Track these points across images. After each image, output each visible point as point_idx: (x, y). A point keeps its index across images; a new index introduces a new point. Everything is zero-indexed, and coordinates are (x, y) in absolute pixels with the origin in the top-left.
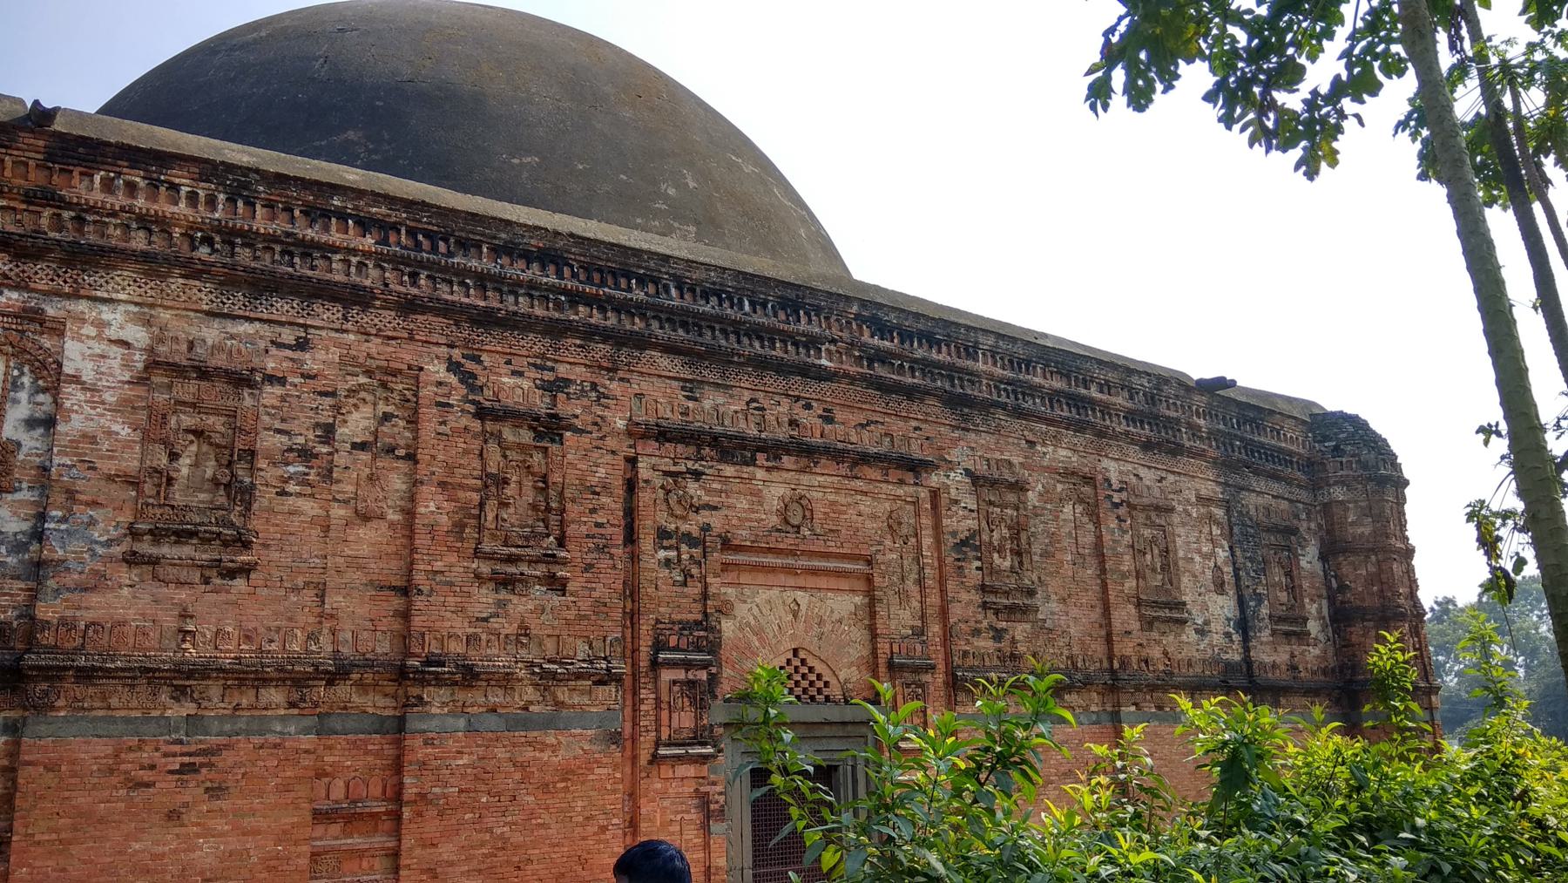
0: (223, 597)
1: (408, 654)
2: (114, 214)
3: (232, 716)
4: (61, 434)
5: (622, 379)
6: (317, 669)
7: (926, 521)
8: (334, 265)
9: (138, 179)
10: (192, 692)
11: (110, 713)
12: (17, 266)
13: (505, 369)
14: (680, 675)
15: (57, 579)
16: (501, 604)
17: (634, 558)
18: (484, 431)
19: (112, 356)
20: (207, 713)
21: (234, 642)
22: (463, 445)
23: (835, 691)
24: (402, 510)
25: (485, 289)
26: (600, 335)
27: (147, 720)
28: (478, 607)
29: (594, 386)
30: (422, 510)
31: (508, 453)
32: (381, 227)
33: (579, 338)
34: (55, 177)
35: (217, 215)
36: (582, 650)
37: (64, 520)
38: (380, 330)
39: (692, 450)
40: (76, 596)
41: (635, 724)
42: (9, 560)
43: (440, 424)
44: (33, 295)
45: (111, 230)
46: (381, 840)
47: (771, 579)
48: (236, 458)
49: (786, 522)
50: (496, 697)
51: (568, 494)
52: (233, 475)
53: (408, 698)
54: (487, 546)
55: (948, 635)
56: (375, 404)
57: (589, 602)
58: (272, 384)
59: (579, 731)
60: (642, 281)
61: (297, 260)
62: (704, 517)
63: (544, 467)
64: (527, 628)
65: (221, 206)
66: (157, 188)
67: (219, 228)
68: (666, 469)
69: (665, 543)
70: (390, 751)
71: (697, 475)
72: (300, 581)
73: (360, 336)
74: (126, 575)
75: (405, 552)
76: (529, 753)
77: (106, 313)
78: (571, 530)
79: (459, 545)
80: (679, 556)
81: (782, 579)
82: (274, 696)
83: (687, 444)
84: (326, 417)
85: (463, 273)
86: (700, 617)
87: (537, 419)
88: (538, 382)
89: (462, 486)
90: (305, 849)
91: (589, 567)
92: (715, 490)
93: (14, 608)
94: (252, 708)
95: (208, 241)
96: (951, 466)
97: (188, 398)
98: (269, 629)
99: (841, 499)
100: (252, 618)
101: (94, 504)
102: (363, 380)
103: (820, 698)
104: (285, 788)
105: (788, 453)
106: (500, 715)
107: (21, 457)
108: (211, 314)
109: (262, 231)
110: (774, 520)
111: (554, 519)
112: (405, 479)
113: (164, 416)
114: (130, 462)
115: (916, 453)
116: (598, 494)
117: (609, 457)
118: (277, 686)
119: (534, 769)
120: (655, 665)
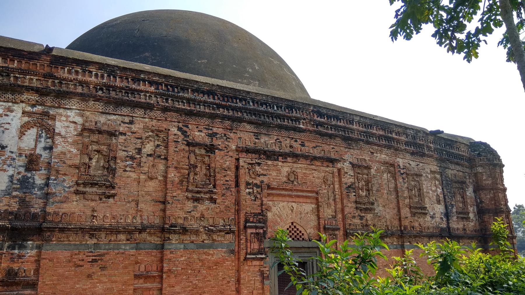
0: (106, 204)
1: (165, 223)
2: (71, 81)
3: (109, 243)
4: (54, 152)
5: (234, 133)
6: (136, 228)
7: (336, 179)
8: (141, 97)
9: (79, 70)
10: (96, 235)
11: (69, 242)
12: (41, 98)
13: (196, 130)
14: (254, 231)
15: (53, 199)
16: (195, 207)
17: (238, 192)
18: (189, 150)
19: (71, 126)
20: (100, 243)
21: (110, 219)
22: (183, 155)
23: (306, 237)
24: (163, 176)
25: (190, 103)
26: (227, 118)
27: (81, 245)
28: (187, 208)
29: (225, 135)
30: (170, 176)
31: (197, 157)
32: (156, 84)
33: (220, 119)
34: (53, 69)
35: (104, 81)
36: (221, 222)
37: (55, 180)
38: (156, 117)
39: (257, 156)
40: (59, 205)
41: (239, 247)
42: (38, 193)
43: (175, 148)
44: (46, 107)
45: (70, 86)
46: (156, 285)
47: (284, 199)
48: (110, 159)
49: (289, 179)
50: (194, 238)
51: (216, 170)
52: (109, 165)
53: (165, 238)
54: (190, 188)
55: (344, 218)
56: (154, 142)
57: (224, 206)
58: (121, 135)
59: (220, 249)
60: (241, 100)
61: (130, 95)
62: (261, 178)
63: (209, 162)
64: (203, 215)
65: (105, 78)
66: (85, 72)
67: (105, 85)
68: (249, 162)
69: (249, 187)
70: (159, 255)
71: (259, 164)
72: (130, 199)
73: (149, 119)
74: (75, 198)
75: (164, 190)
76: (204, 257)
77: (69, 113)
78: (218, 183)
79: (181, 187)
80: (253, 191)
81: (288, 199)
82: (122, 237)
83: (256, 154)
84: (139, 146)
85: (182, 98)
86: (260, 211)
87: (207, 146)
88: (207, 134)
89: (182, 168)
90: (132, 287)
91: (224, 195)
92: (265, 169)
93: (40, 208)
94: (115, 241)
95: (101, 89)
96: (345, 161)
97: (95, 140)
98: (121, 215)
99: (307, 172)
100: (115, 211)
101: (65, 174)
102: (150, 134)
103: (301, 239)
104: (125, 267)
105: (289, 157)
106: (195, 244)
107: (42, 159)
108: (102, 113)
109: (119, 86)
110: (285, 179)
111: (212, 179)
112: (164, 166)
113: (87, 146)
114: (77, 161)
115: (333, 156)
116: (227, 170)
117: (230, 158)
118: (123, 234)
119: (206, 262)
120: (245, 227)
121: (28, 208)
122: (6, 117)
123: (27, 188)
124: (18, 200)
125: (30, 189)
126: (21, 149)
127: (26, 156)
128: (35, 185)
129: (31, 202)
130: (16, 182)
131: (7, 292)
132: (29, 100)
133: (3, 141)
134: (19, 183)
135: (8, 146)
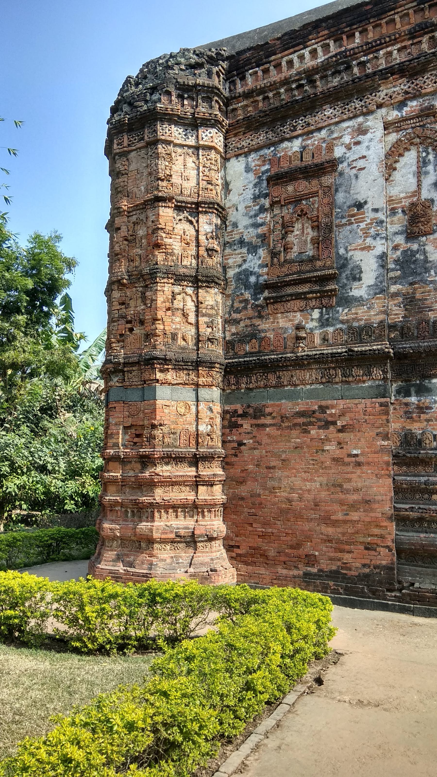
12: (413, 83)
34: (427, 13)
121: (421, 312)
122: (358, 147)
123: (414, 273)
124: (401, 299)
125: (420, 274)
126: (393, 200)
127: (403, 211)
128: (429, 265)
129: (426, 299)
130: (393, 266)
131: (409, 476)
132: (391, 97)
133: (357, 193)
134: (398, 267)
135: (368, 200)
